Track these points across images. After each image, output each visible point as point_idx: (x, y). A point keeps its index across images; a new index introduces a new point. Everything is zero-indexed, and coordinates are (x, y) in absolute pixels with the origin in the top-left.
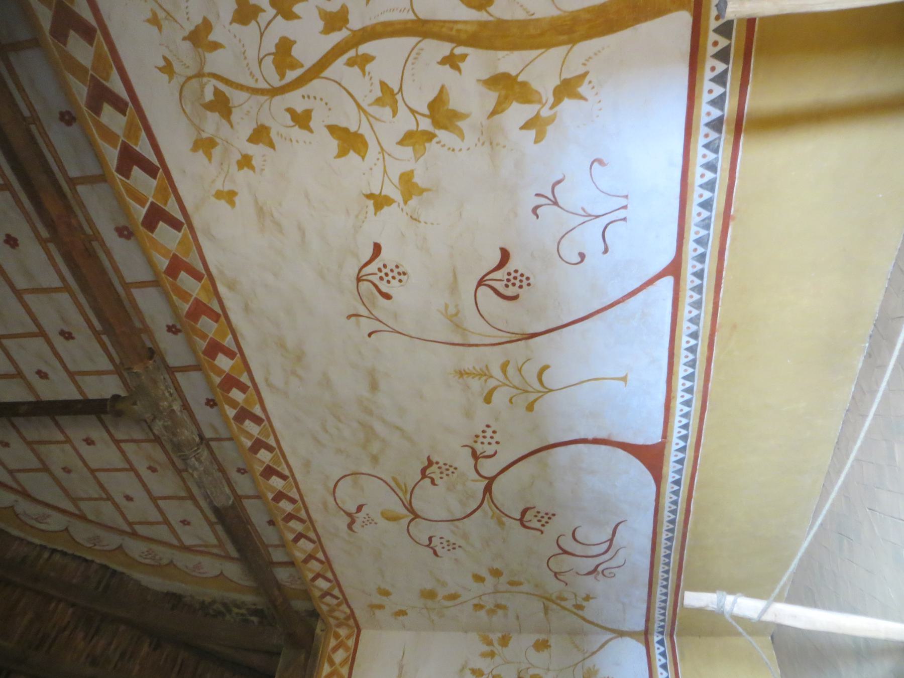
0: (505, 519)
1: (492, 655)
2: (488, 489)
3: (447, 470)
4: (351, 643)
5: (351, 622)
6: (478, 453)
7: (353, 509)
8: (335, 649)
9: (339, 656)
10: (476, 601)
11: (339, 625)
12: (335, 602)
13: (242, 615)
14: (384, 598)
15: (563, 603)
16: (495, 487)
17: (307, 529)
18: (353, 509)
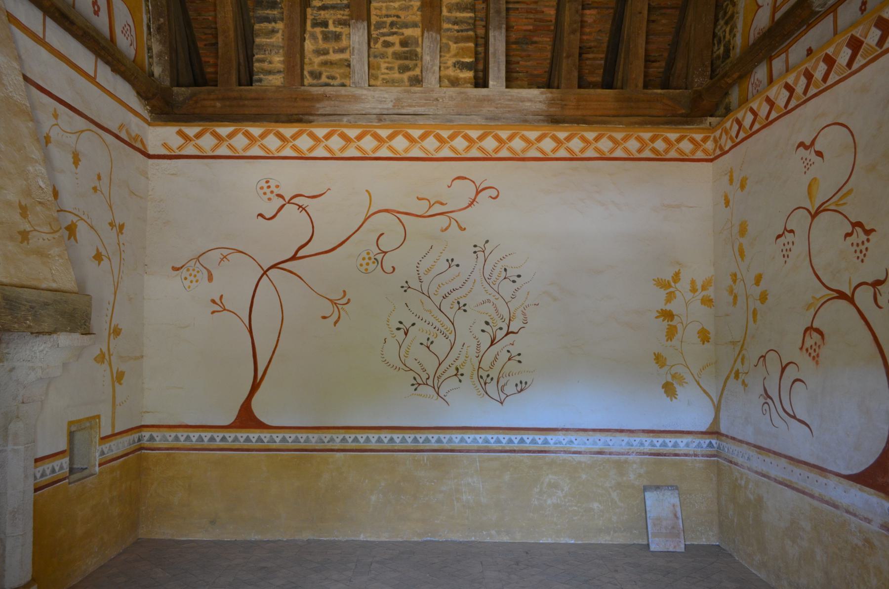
0: (812, 311)
1: (694, 290)
2: (841, 295)
3: (861, 252)
4: (699, 155)
5: (718, 152)
6: (879, 287)
7: (817, 147)
8: (692, 140)
9: (686, 146)
10: (739, 276)
11: (715, 141)
12: (734, 134)
13: (724, 37)
14: (739, 185)
15: (739, 360)
16: (843, 303)
17: (798, 99)
18: (817, 147)
